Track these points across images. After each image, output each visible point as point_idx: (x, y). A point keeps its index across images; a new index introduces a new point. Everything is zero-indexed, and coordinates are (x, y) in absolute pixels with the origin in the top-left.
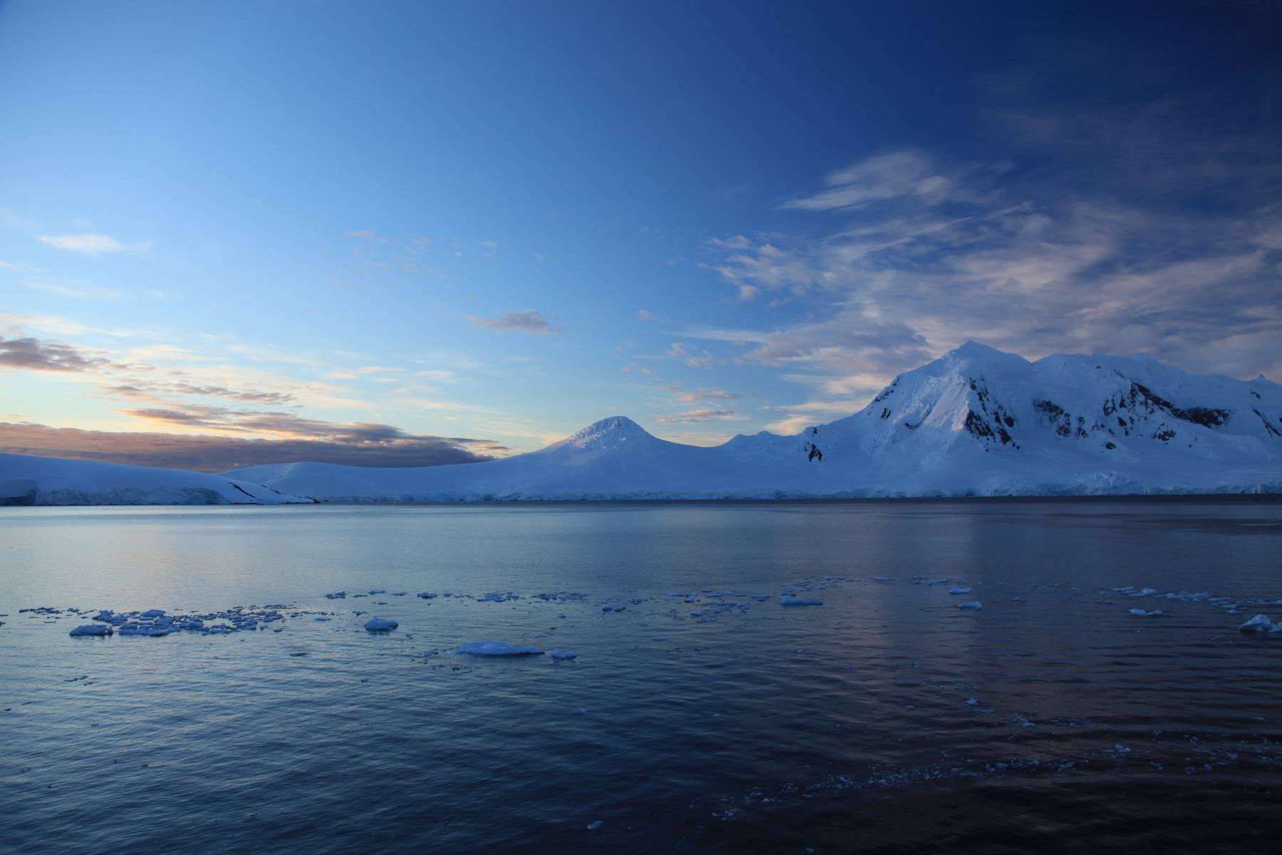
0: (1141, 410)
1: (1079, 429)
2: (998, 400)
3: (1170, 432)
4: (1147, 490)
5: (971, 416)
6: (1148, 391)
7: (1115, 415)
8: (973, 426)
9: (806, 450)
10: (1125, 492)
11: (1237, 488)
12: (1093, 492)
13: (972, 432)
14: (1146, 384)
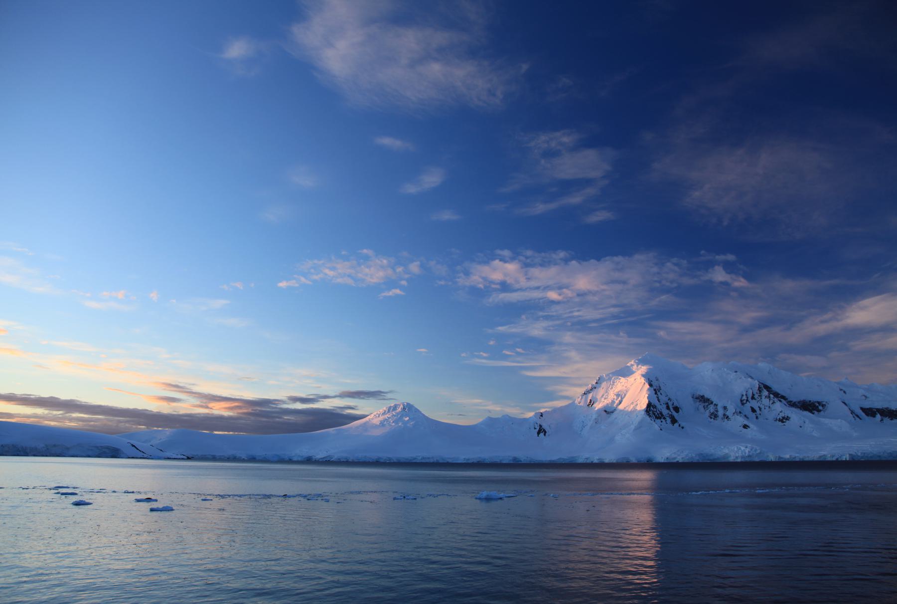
0: (766, 401)
1: (724, 415)
2: (668, 394)
3: (786, 417)
4: (772, 457)
5: (649, 405)
6: (770, 388)
7: (748, 405)
8: (651, 412)
9: (535, 429)
10: (757, 459)
11: (833, 456)
12: (735, 459)
13: (650, 416)
14: (768, 383)
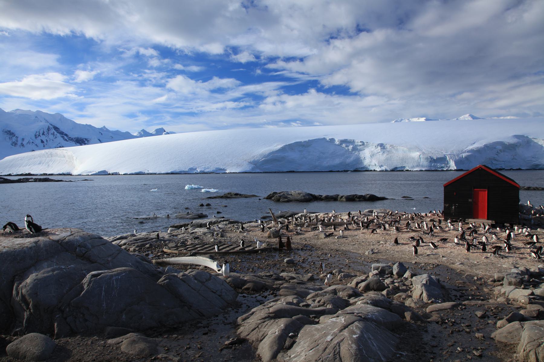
0: (51, 137)
1: (22, 143)
6: (59, 129)
